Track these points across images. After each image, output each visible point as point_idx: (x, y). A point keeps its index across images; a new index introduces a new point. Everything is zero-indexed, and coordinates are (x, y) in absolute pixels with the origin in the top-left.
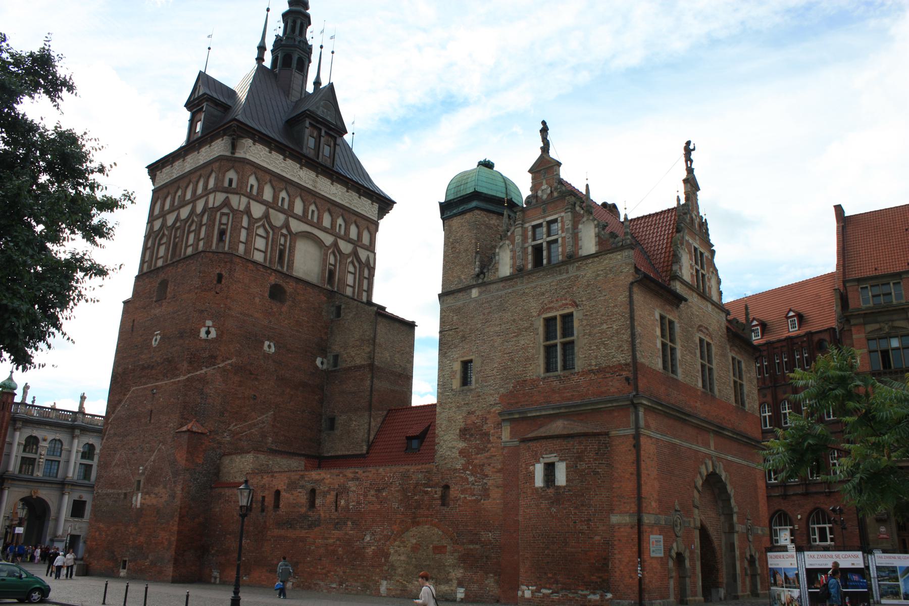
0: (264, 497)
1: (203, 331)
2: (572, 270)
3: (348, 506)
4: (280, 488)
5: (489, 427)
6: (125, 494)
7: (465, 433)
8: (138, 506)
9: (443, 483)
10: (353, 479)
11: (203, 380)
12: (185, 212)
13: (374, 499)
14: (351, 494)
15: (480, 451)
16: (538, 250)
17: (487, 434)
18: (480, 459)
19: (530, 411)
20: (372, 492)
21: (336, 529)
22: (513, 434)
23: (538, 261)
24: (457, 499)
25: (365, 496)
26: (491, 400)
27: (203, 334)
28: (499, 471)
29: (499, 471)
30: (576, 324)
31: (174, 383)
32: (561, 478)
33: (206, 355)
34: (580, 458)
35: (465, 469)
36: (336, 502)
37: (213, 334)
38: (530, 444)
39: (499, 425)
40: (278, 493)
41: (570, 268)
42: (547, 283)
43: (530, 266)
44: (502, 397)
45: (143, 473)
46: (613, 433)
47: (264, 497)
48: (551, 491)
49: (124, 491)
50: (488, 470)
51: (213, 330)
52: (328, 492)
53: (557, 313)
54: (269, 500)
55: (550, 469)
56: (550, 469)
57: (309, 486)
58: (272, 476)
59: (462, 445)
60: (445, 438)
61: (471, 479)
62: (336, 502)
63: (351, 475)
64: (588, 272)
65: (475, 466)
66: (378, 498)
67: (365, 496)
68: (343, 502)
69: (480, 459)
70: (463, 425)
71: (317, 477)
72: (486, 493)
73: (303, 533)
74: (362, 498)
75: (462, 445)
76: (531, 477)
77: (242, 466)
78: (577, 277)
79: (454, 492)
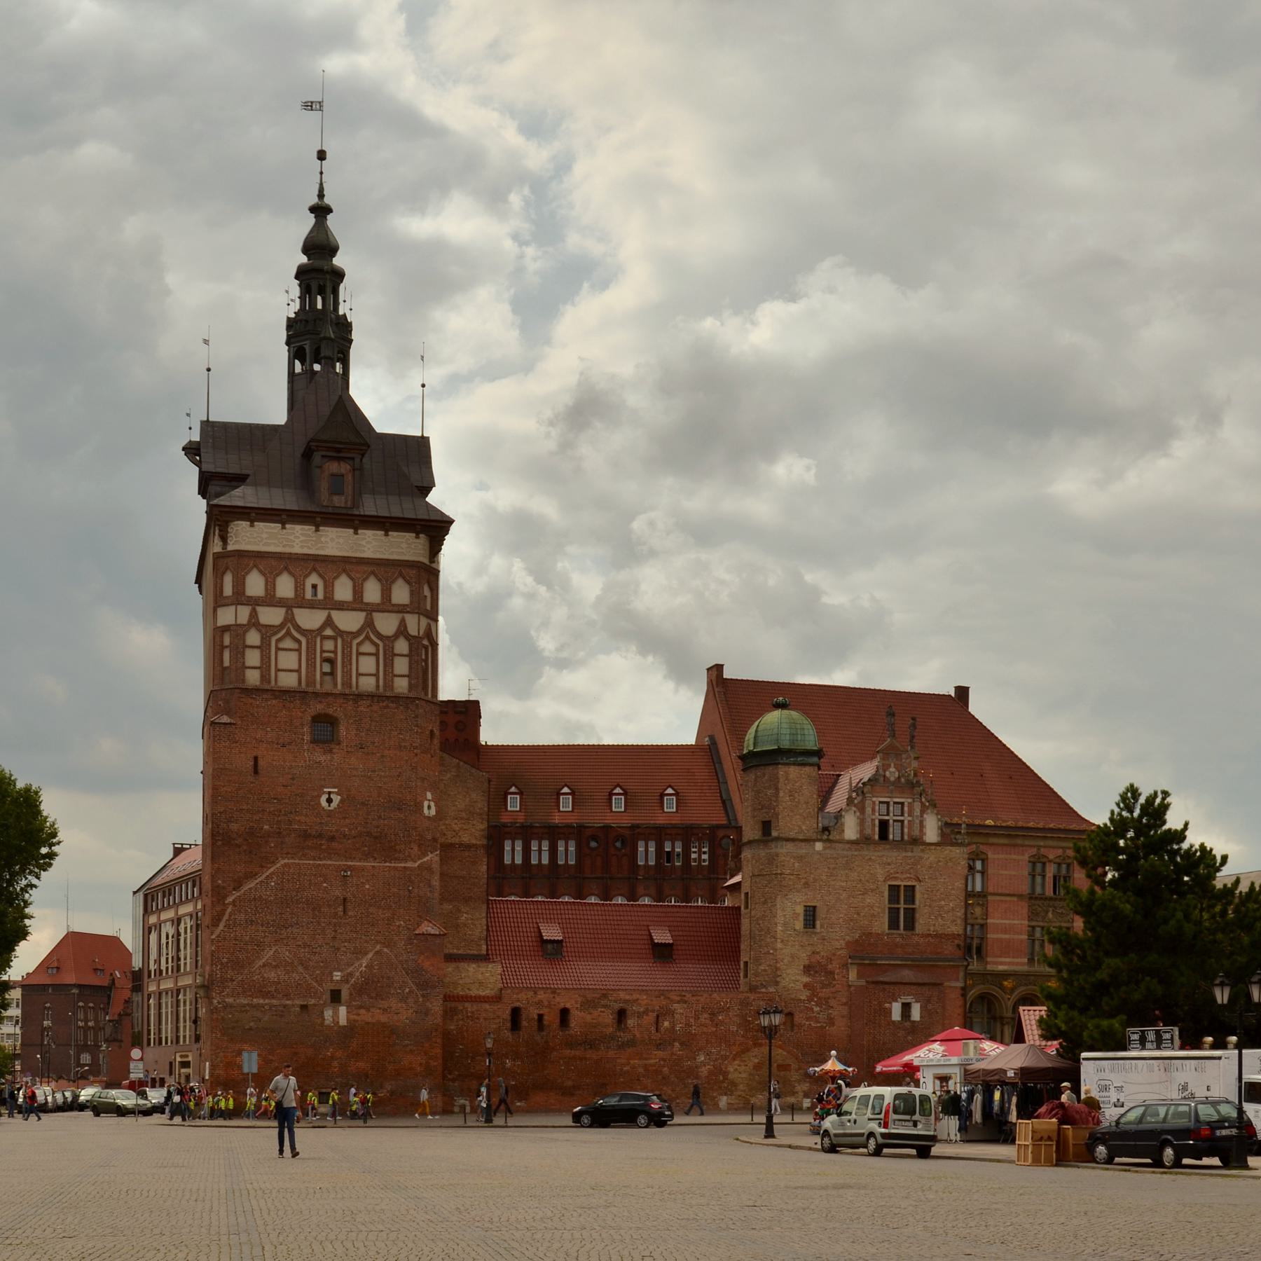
0: (541, 1016)
1: (426, 804)
2: (917, 851)
3: (673, 1027)
4: (568, 1006)
5: (834, 966)
6: (304, 1007)
7: (808, 969)
8: (343, 1020)
9: (786, 1011)
10: (678, 1002)
11: (426, 868)
12: (350, 621)
13: (708, 1021)
14: (677, 1016)
15: (824, 986)
16: (884, 825)
17: (832, 973)
18: (825, 993)
19: (881, 959)
20: (706, 1016)
21: (658, 1049)
22: (860, 976)
23: (884, 834)
24: (800, 1026)
25: (697, 1018)
26: (837, 945)
27: (426, 811)
28: (845, 1004)
29: (845, 1004)
30: (918, 896)
31: (395, 868)
32: (916, 1014)
33: (429, 837)
34: (929, 1001)
35: (810, 1000)
36: (657, 1023)
37: (433, 812)
38: (886, 986)
39: (845, 966)
40: (565, 1013)
41: (915, 849)
42: (894, 856)
43: (877, 837)
44: (848, 943)
45: (345, 980)
46: (946, 984)
47: (541, 1016)
48: (907, 1024)
49: (299, 1002)
50: (832, 1002)
51: (432, 804)
52: (646, 1012)
53: (903, 884)
54: (552, 1018)
55: (906, 1007)
56: (906, 1007)
57: (617, 1006)
58: (554, 992)
59: (806, 979)
60: (789, 971)
61: (816, 1009)
62: (657, 1023)
63: (678, 998)
64: (931, 857)
65: (820, 998)
66: (712, 1020)
67: (697, 1018)
68: (666, 1024)
69: (825, 993)
70: (807, 962)
71: (628, 997)
72: (831, 1021)
73: (611, 1054)
74: (692, 1020)
75: (806, 979)
76: (889, 1012)
77: (480, 977)
78: (921, 858)
79: (798, 1019)
